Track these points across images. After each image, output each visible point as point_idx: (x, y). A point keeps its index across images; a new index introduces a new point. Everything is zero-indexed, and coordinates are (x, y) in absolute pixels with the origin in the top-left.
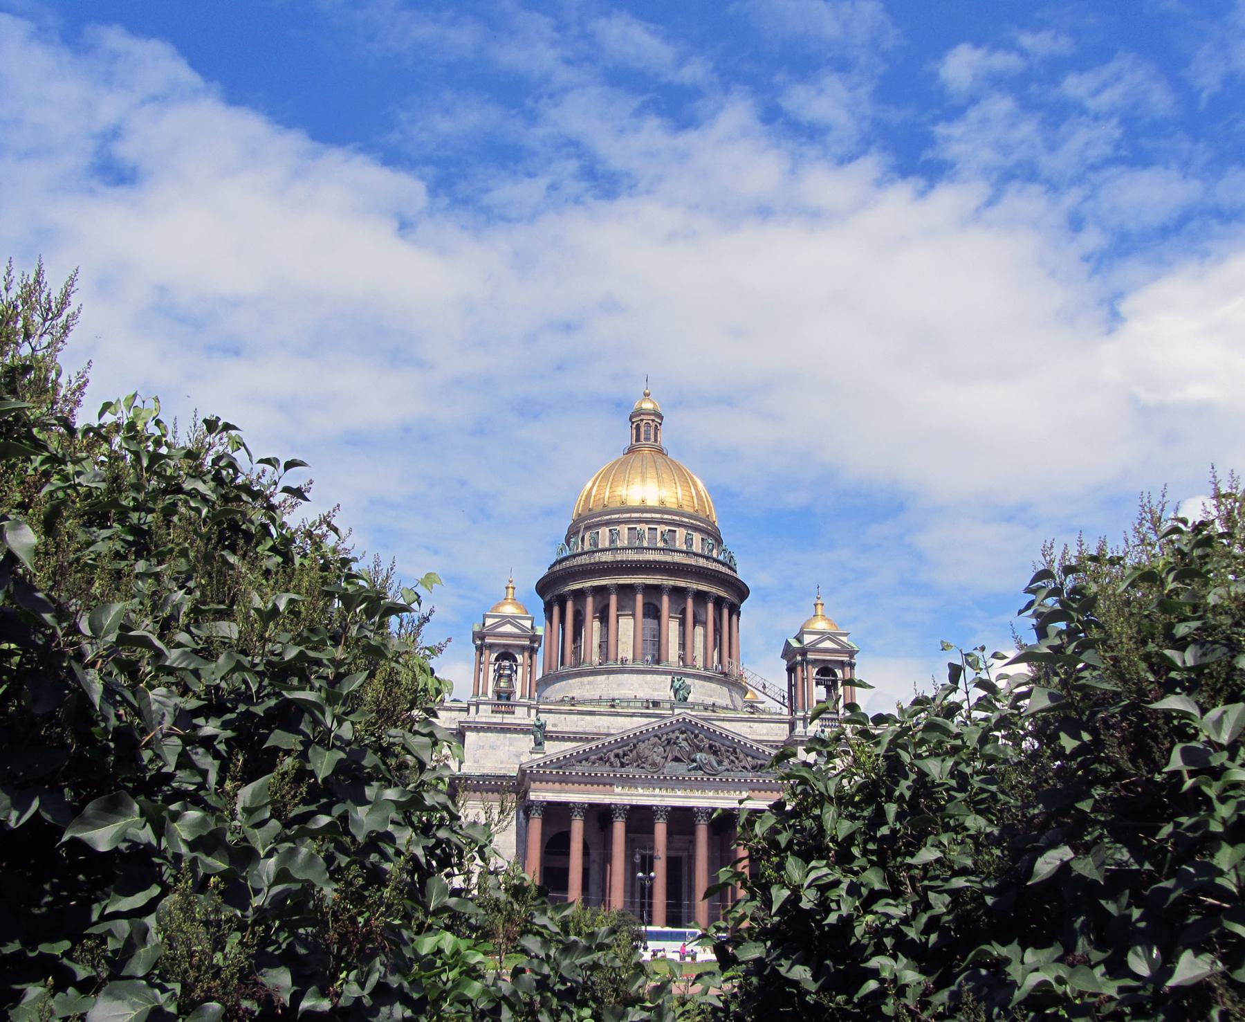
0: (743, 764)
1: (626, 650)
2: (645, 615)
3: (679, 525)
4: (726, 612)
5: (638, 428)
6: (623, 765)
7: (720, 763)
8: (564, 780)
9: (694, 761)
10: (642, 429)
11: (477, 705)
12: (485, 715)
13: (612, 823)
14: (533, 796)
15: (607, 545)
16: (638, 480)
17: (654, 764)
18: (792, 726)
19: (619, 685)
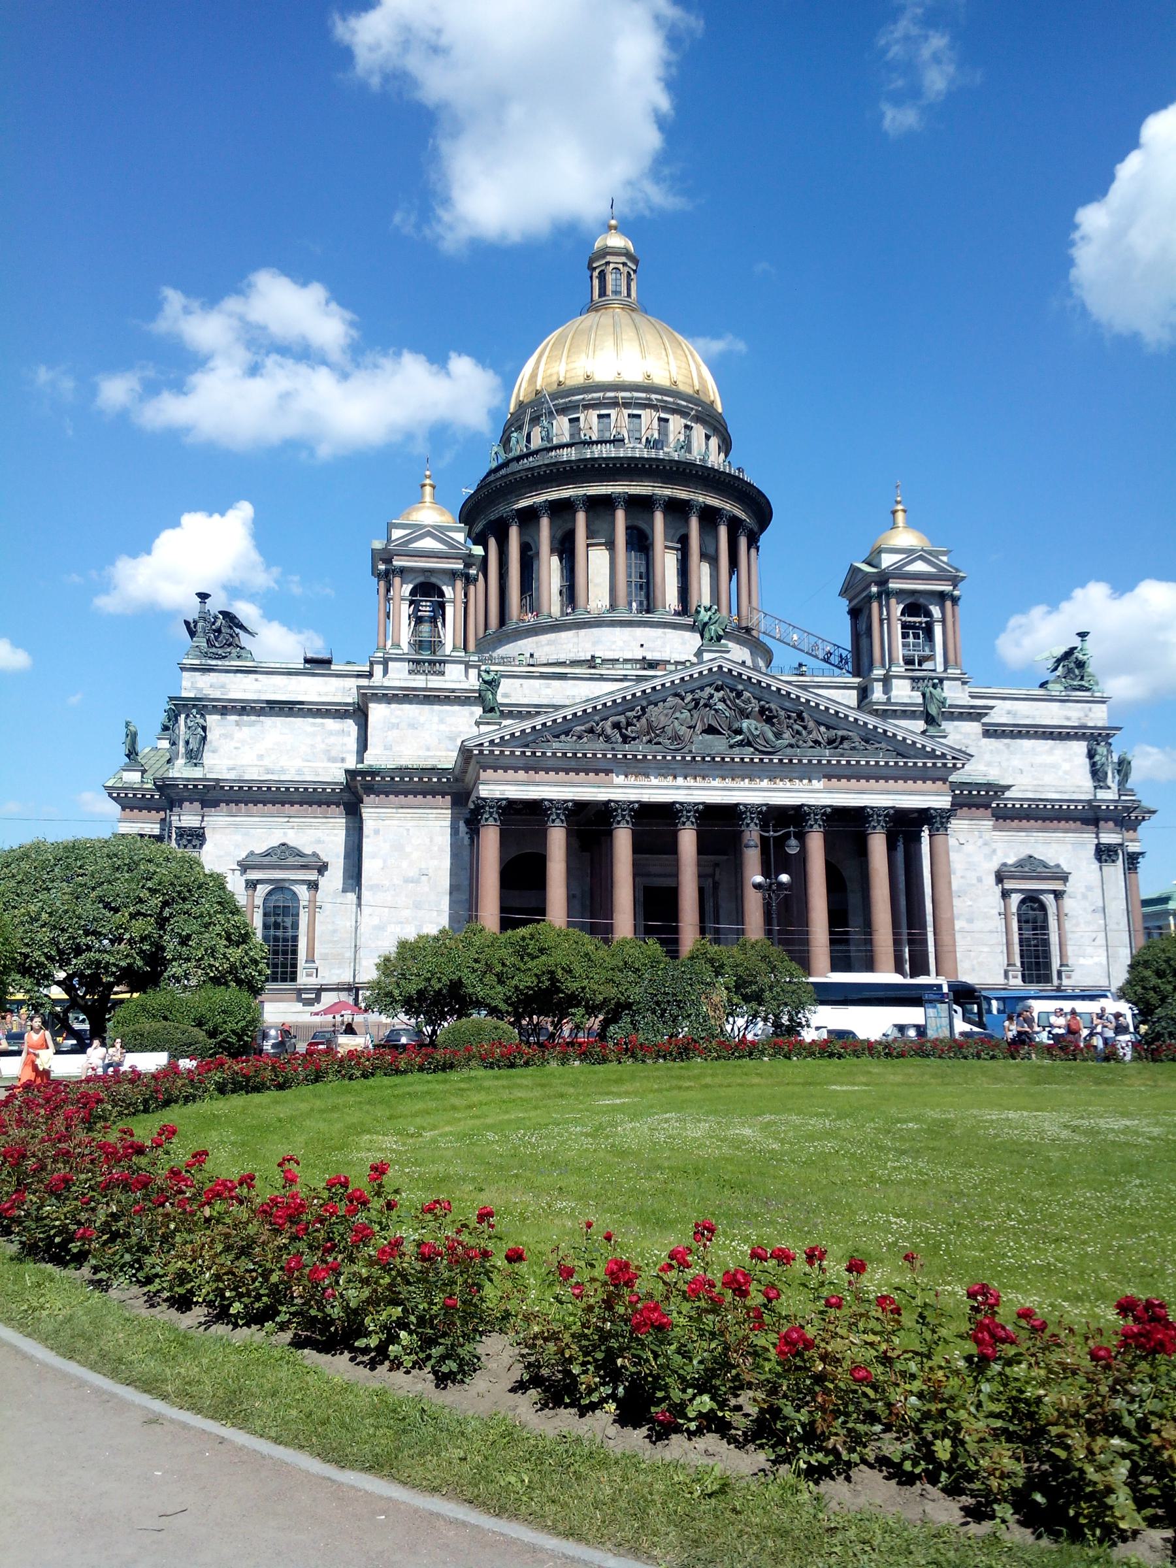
0: (814, 735)
1: (597, 597)
2: (630, 545)
3: (674, 411)
4: (743, 542)
5: (602, 276)
6: (625, 739)
7: (778, 735)
8: (533, 766)
9: (739, 732)
10: (610, 278)
11: (385, 663)
12: (399, 676)
13: (609, 834)
14: (484, 791)
15: (566, 439)
16: (609, 343)
17: (676, 737)
18: (864, 693)
19: (594, 644)
